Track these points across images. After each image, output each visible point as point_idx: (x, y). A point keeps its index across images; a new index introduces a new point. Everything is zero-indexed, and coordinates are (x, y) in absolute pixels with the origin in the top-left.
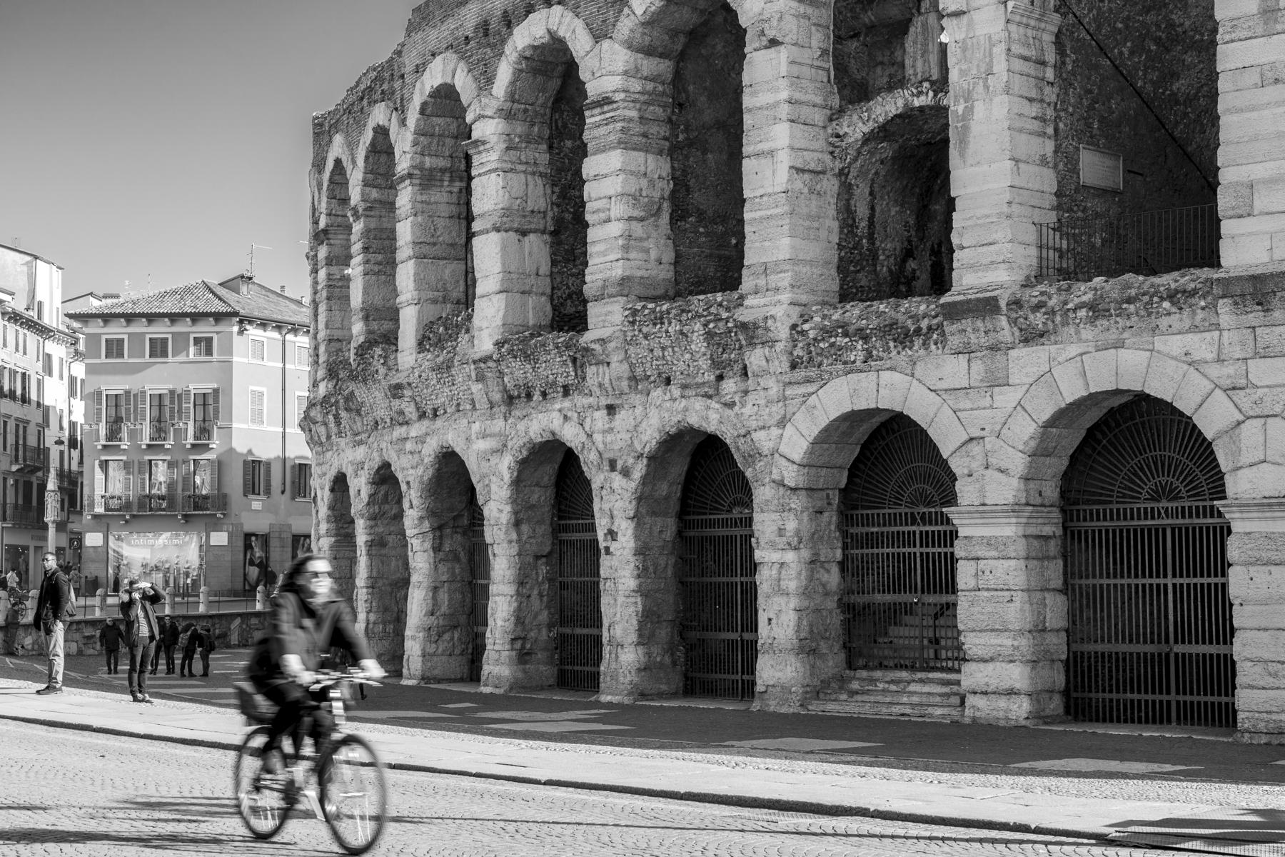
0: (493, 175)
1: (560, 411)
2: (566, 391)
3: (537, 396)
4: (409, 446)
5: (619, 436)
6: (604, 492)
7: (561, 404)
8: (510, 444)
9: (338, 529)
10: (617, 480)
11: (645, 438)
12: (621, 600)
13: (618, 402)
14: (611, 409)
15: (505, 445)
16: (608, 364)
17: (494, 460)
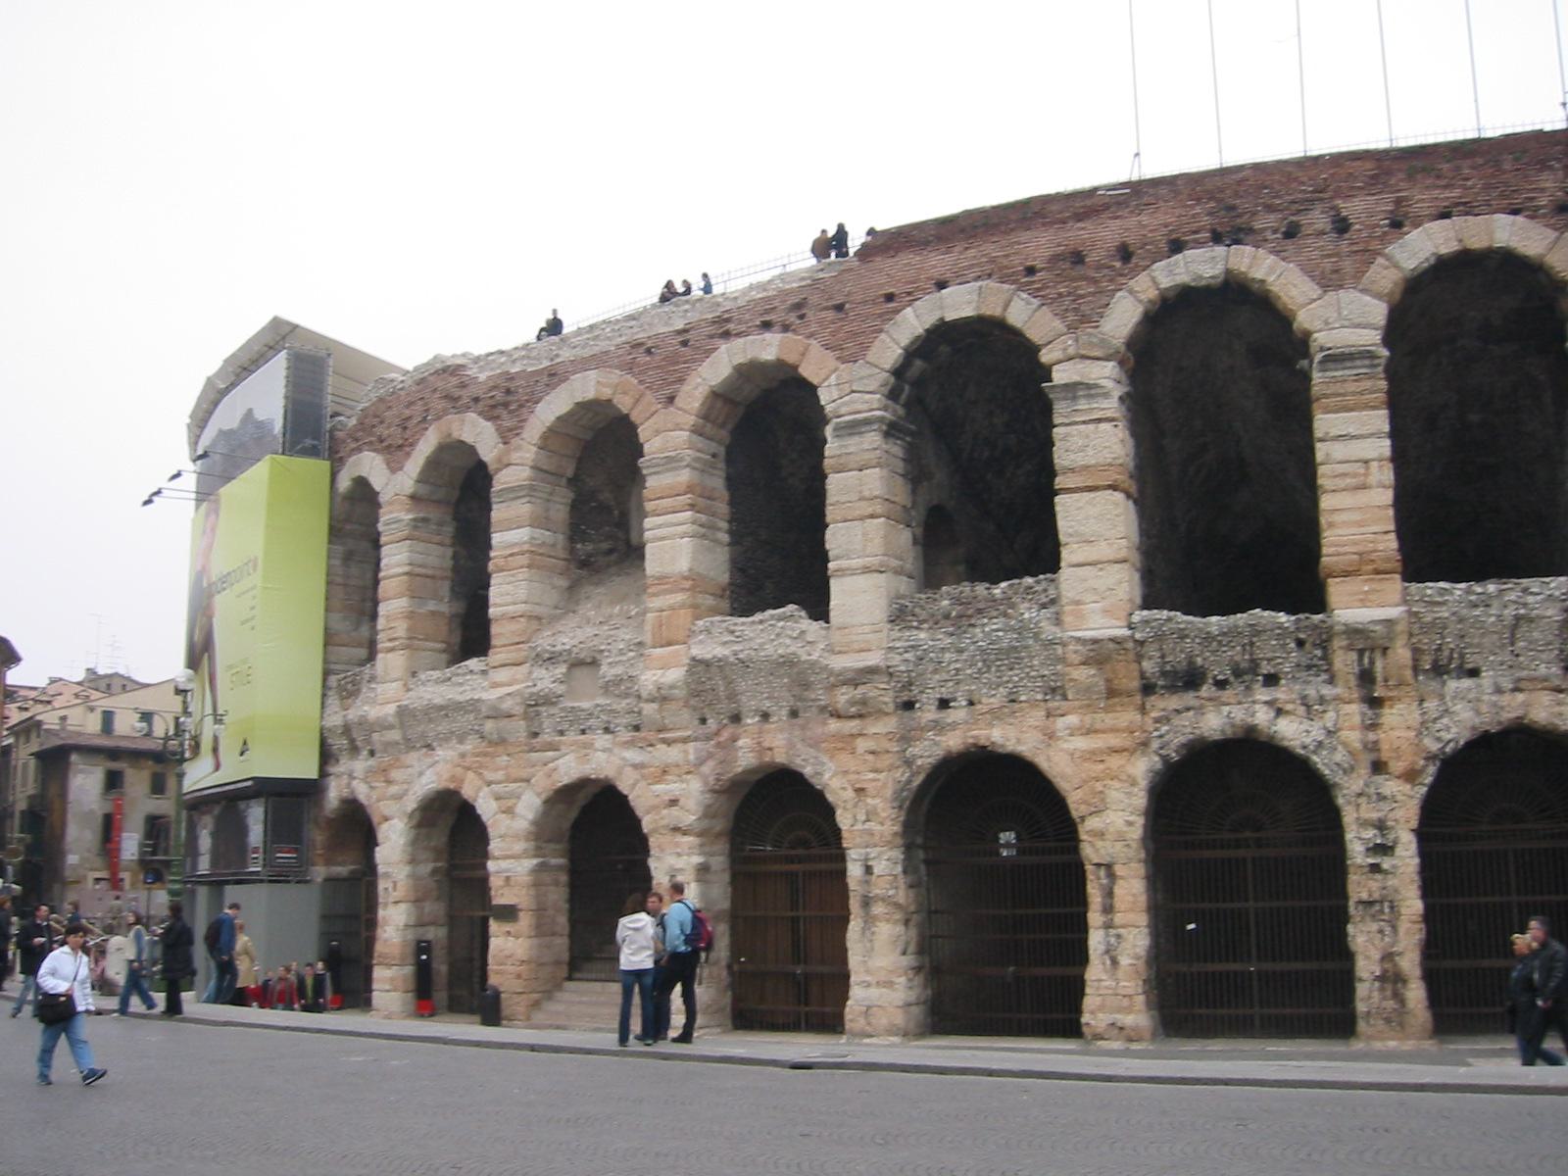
0: (1103, 426)
1: (1266, 703)
2: (1272, 680)
3: (1206, 690)
4: (862, 745)
5: (1397, 733)
6: (1363, 800)
7: (1262, 694)
8: (1155, 745)
9: (538, 848)
10: (1391, 786)
11: (1447, 736)
12: (1404, 926)
13: (1391, 694)
14: (1375, 703)
15: (1145, 744)
16: (1385, 650)
17: (1115, 762)
